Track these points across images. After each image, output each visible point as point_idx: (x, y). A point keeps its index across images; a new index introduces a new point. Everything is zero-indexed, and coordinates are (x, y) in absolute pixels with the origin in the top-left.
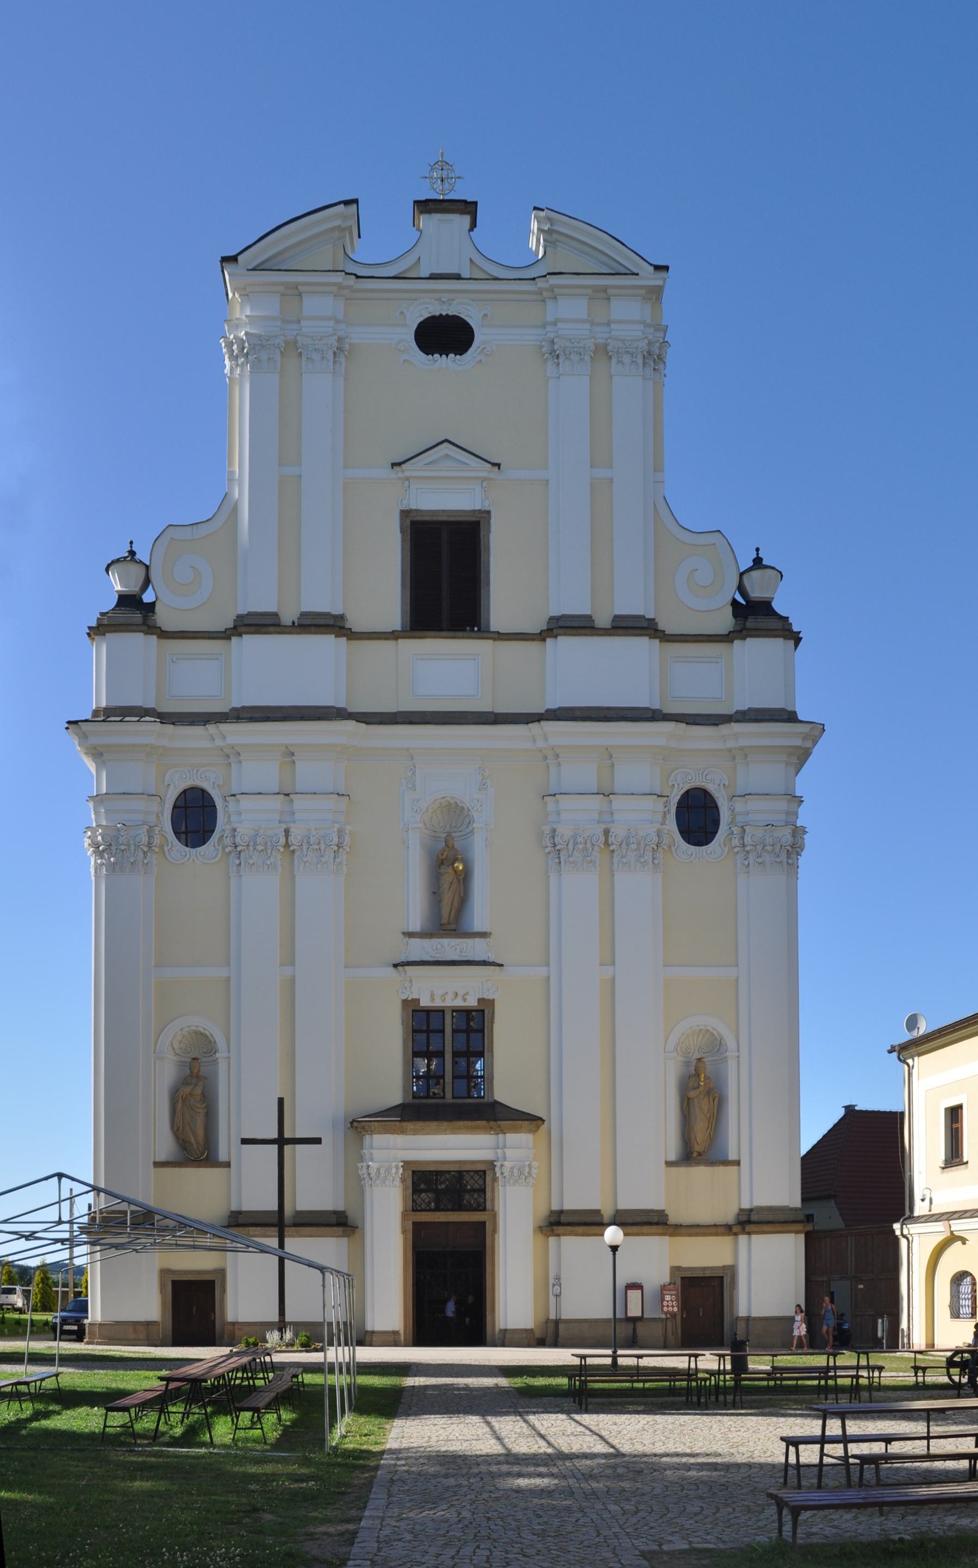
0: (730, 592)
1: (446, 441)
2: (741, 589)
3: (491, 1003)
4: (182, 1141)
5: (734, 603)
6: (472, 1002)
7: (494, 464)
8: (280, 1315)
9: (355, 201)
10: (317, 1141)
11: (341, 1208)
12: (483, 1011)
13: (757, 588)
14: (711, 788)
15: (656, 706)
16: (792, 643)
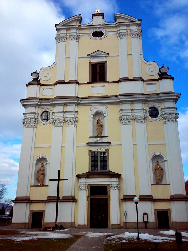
0: (157, 71)
1: (98, 50)
2: (160, 71)
3: (109, 150)
4: (37, 179)
5: (159, 74)
6: (104, 150)
7: (108, 54)
8: (56, 221)
9: (81, 15)
10: (67, 180)
11: (73, 195)
12: (107, 152)
13: (163, 71)
14: (156, 107)
15: (143, 92)
16: (172, 80)
